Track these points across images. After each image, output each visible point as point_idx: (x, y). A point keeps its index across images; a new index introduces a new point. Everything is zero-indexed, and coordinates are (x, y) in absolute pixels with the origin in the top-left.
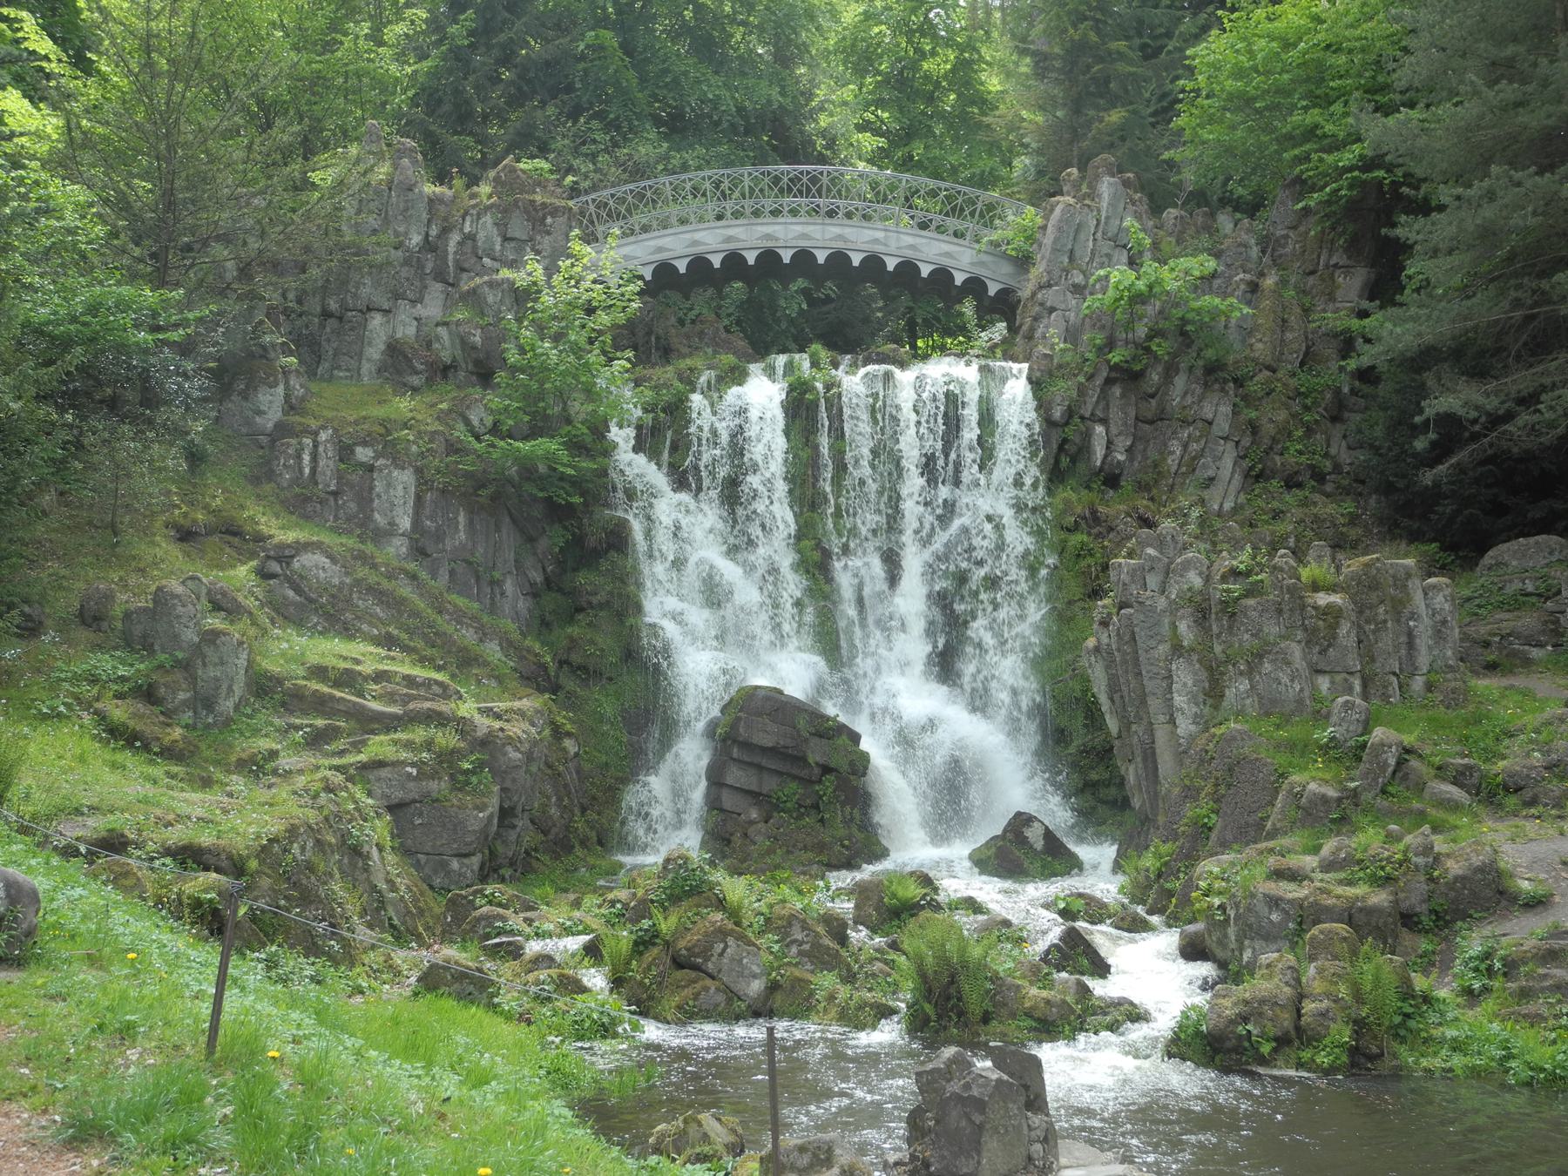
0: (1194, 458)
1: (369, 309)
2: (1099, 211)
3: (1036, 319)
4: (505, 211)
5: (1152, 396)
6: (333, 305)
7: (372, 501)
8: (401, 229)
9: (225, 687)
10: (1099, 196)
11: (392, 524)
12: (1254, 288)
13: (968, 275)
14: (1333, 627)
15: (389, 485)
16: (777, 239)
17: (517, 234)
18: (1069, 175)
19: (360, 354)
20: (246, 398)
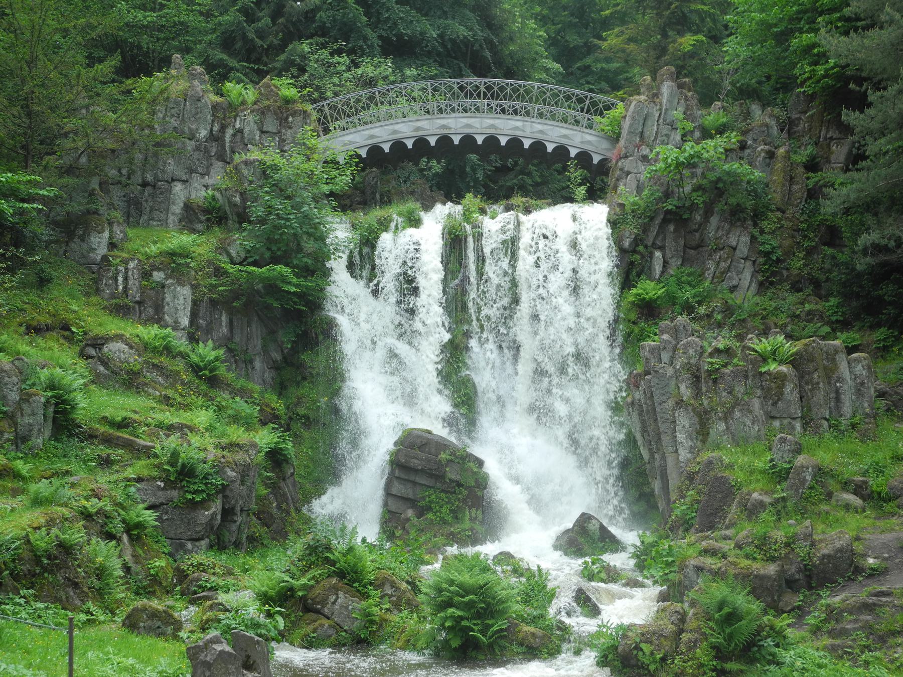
0: (722, 273)
1: (173, 180)
2: (661, 105)
3: (618, 180)
4: (263, 113)
5: (696, 231)
6: (149, 178)
7: (164, 307)
8: (194, 127)
9: (36, 429)
10: (662, 95)
12: (771, 155)
13: (579, 150)
14: (781, 387)
15: (174, 297)
16: (450, 128)
17: (270, 129)
18: (644, 80)
19: (167, 210)
20: (83, 240)
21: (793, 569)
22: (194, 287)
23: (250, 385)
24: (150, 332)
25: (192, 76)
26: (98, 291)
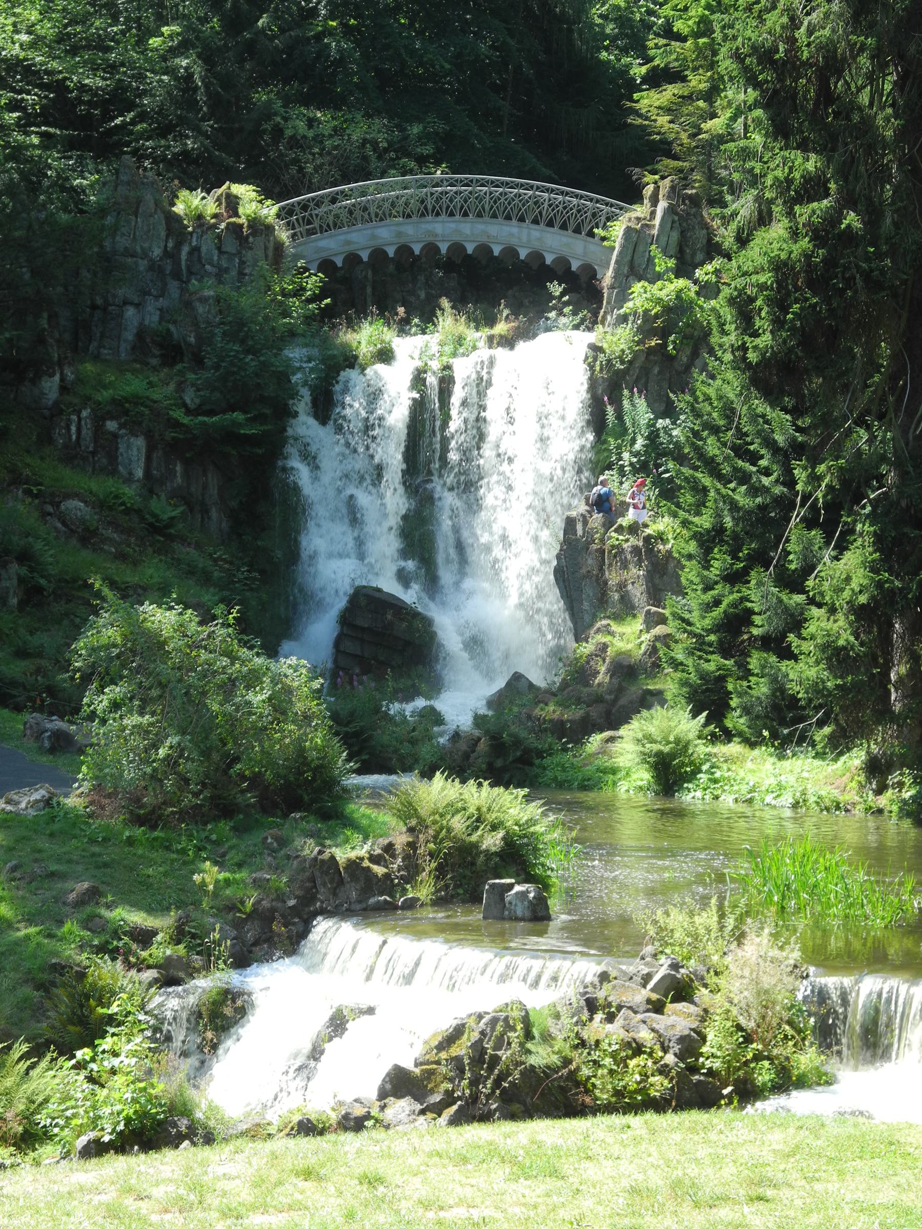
7: (117, 457)
8: (146, 245)
11: (130, 474)
16: (436, 236)
19: (119, 337)
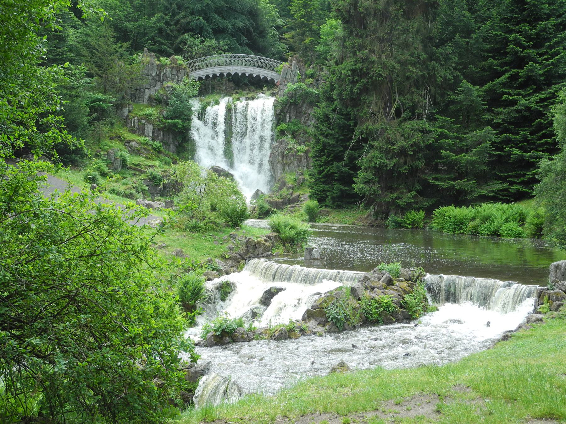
21: (286, 200)
22: (153, 125)
23: (170, 153)
24: (142, 139)
25: (151, 56)
26: (126, 126)
